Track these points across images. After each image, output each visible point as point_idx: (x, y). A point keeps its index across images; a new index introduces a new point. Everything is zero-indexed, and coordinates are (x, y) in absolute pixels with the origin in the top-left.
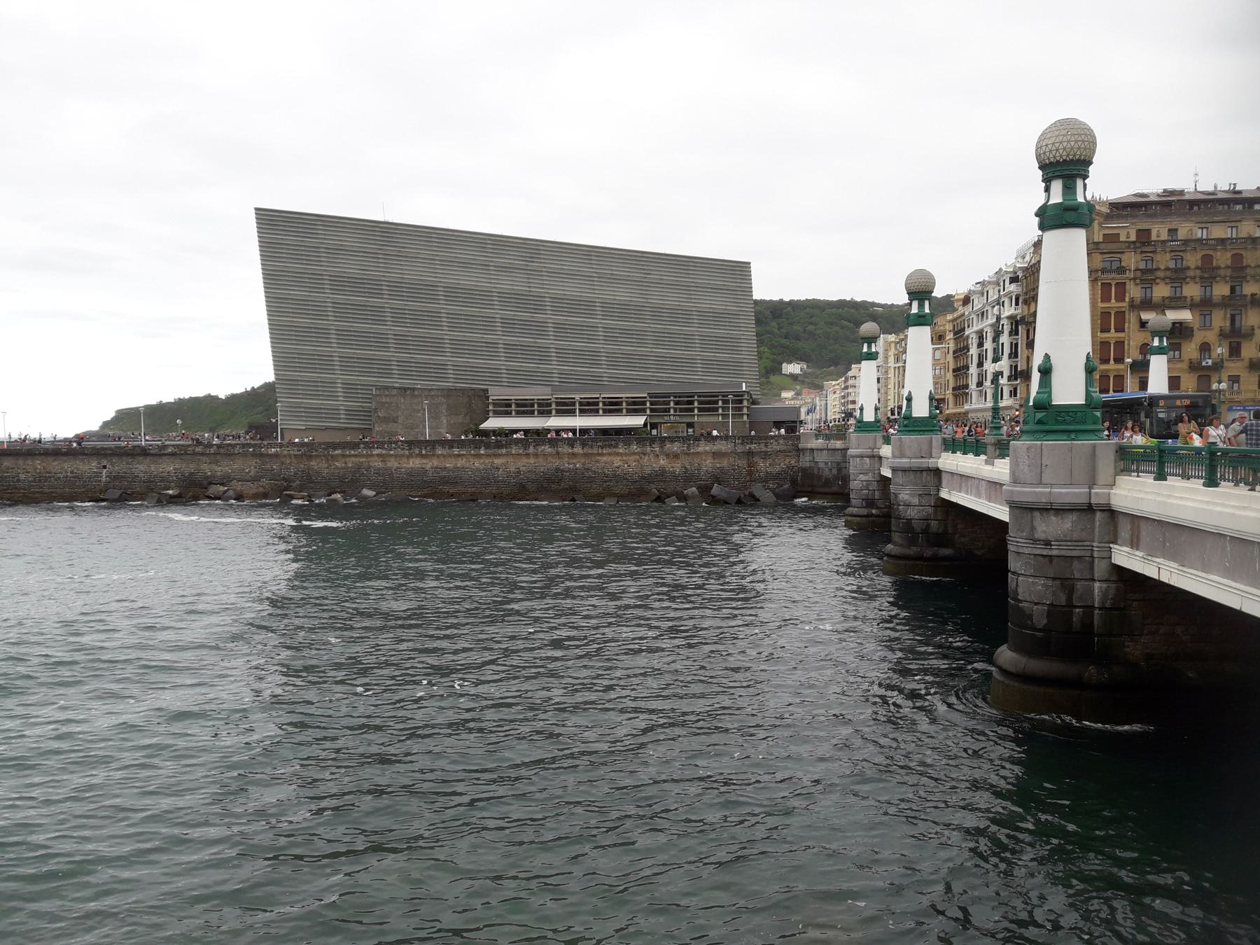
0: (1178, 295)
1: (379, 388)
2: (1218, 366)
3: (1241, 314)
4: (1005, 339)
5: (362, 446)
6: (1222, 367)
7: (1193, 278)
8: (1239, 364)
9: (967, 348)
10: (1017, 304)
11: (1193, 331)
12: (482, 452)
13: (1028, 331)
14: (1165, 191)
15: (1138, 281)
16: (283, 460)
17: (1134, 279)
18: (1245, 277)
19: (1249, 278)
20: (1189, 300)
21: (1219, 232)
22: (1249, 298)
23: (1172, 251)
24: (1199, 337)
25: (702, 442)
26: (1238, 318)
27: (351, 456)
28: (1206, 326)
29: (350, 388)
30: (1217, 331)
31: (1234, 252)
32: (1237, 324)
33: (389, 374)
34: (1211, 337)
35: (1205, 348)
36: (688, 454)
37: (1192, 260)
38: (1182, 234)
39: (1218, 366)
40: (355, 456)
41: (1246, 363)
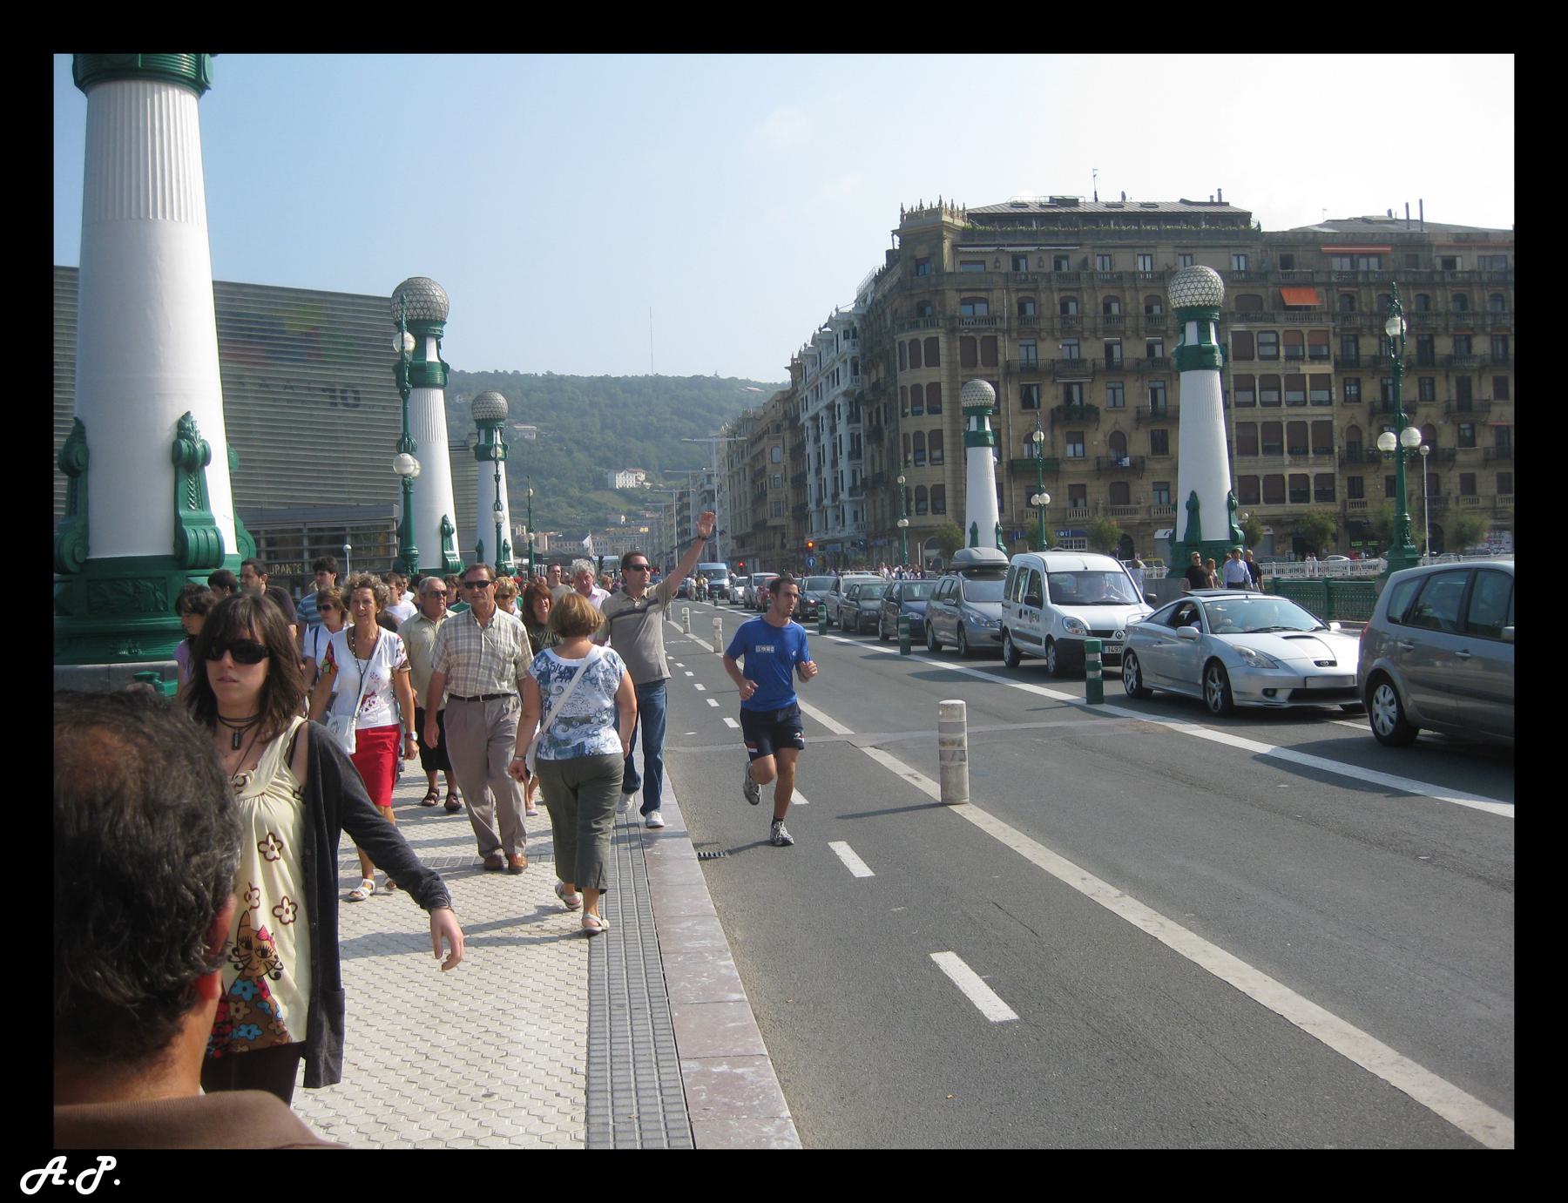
0: (1075, 356)
2: (1138, 467)
3: (1164, 388)
4: (842, 428)
6: (1143, 470)
11: (1098, 414)
20: (1089, 365)
24: (1107, 423)
26: (1160, 393)
28: (1116, 406)
32: (1161, 402)
34: (1124, 421)
35: (1118, 441)
37: (1090, 303)
39: (1138, 467)
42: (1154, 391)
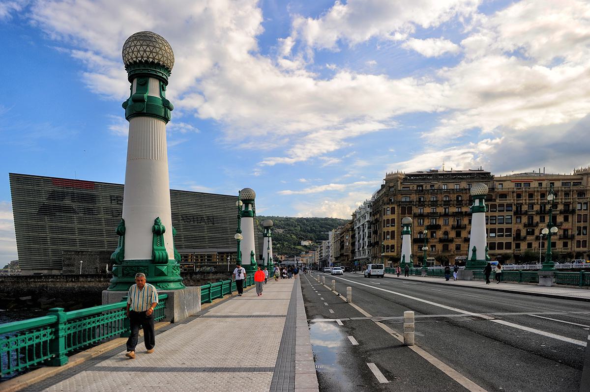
0: (435, 211)
1: (65, 251)
3: (461, 220)
4: (366, 230)
5: (44, 277)
7: (441, 205)
8: (460, 240)
9: (355, 235)
10: (371, 216)
12: (102, 280)
13: (374, 227)
14: (430, 170)
15: (417, 206)
16: (6, 284)
17: (416, 205)
18: (462, 205)
19: (464, 205)
21: (451, 186)
22: (464, 213)
23: (431, 194)
24: (443, 229)
25: (211, 275)
27: (38, 282)
28: (446, 224)
29: (54, 251)
30: (451, 226)
31: (458, 194)
32: (459, 224)
33: (75, 245)
34: (448, 228)
35: (446, 233)
36: (204, 280)
38: (436, 187)
40: (41, 282)
41: (463, 239)
42: (458, 221)
